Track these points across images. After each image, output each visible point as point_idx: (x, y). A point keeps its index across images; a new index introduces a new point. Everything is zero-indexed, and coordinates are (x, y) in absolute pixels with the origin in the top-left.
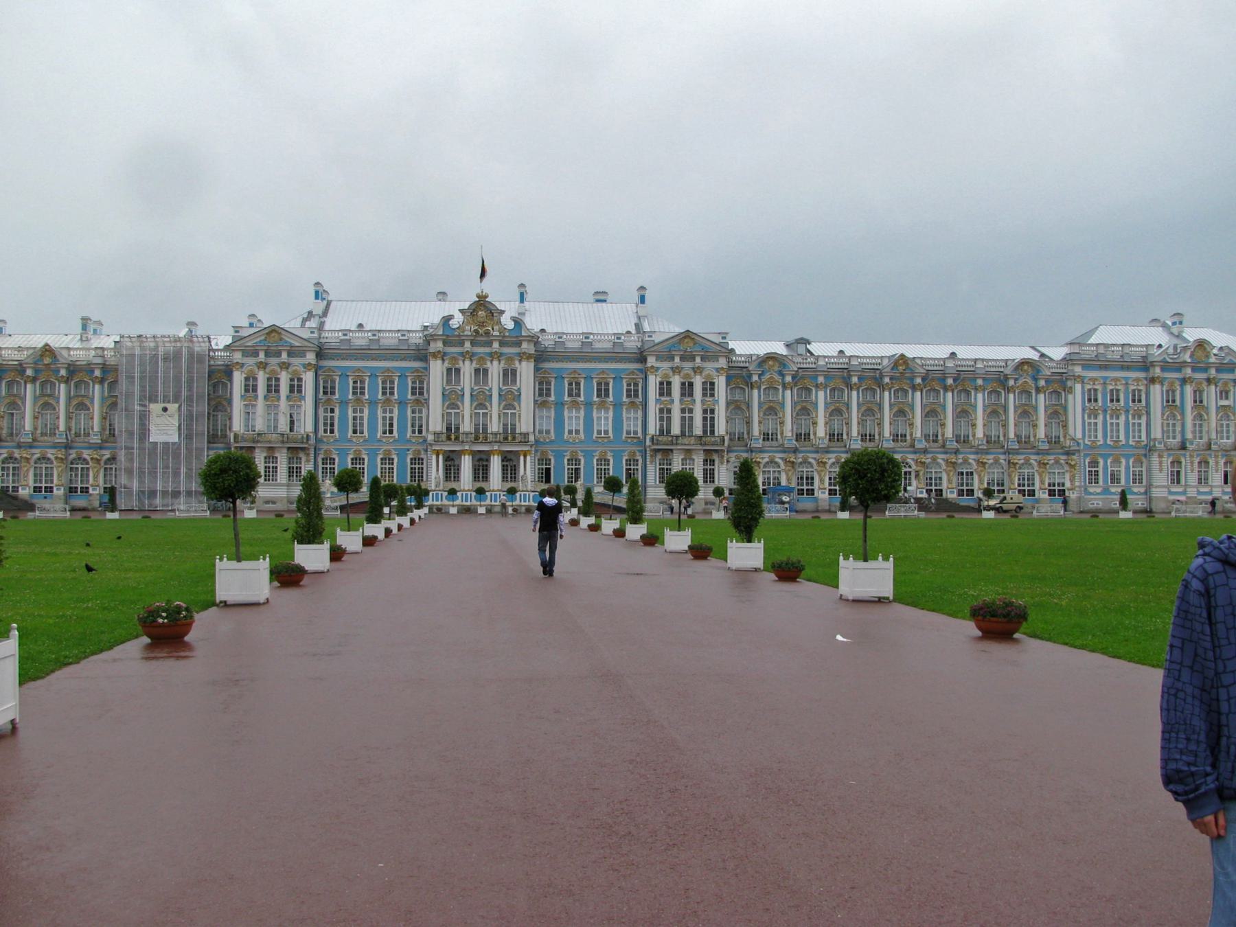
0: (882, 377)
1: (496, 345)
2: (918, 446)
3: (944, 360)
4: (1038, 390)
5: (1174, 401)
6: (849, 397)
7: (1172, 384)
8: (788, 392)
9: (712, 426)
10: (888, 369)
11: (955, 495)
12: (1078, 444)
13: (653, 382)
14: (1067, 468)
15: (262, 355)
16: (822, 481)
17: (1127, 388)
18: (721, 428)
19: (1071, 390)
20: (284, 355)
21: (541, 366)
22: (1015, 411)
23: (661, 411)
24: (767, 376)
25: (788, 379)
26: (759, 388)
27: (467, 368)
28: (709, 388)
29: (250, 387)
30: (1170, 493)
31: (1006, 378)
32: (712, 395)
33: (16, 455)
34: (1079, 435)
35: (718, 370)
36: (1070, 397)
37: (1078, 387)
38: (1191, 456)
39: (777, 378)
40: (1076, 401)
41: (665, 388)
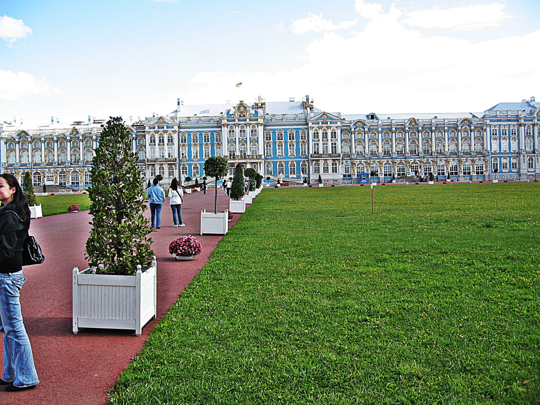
1: (248, 120)
5: (530, 133)
7: (529, 126)
9: (336, 150)
10: (408, 124)
12: (489, 153)
13: (311, 132)
15: (156, 127)
17: (509, 129)
18: (339, 151)
19: (485, 130)
20: (165, 127)
21: (266, 128)
23: (315, 145)
24: (358, 129)
26: (355, 134)
27: (237, 130)
28: (334, 135)
29: (153, 141)
30: (528, 172)
32: (335, 137)
33: (65, 171)
34: (489, 149)
35: (337, 127)
36: (485, 133)
37: (488, 129)
38: (537, 156)
40: (487, 135)
41: (316, 135)
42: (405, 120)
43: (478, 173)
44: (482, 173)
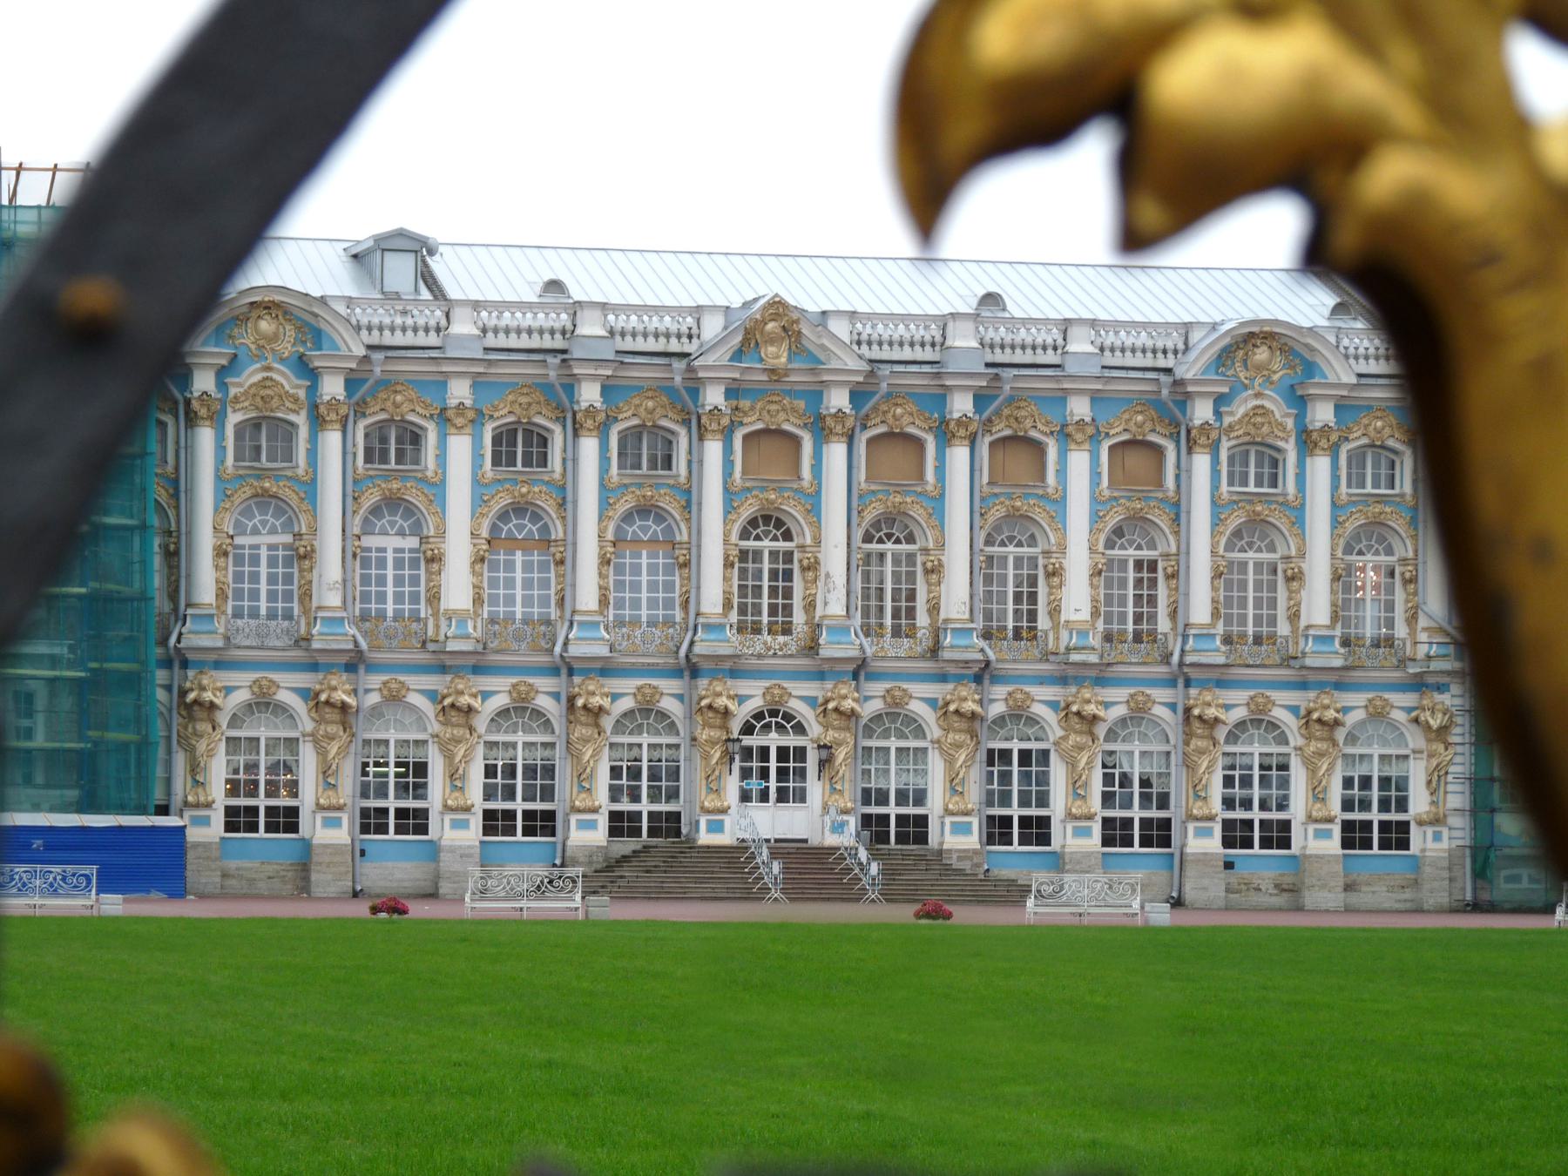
0: (694, 386)
2: (831, 648)
3: (944, 321)
4: (1308, 441)
6: (572, 461)
8: (332, 440)
10: (720, 357)
11: (972, 841)
14: (1415, 739)
16: (455, 778)
22: (1217, 522)
24: (250, 376)
25: (333, 387)
26: (217, 419)
31: (1182, 394)
39: (288, 381)
42: (698, 311)
43: (1355, 835)
44: (1396, 836)
